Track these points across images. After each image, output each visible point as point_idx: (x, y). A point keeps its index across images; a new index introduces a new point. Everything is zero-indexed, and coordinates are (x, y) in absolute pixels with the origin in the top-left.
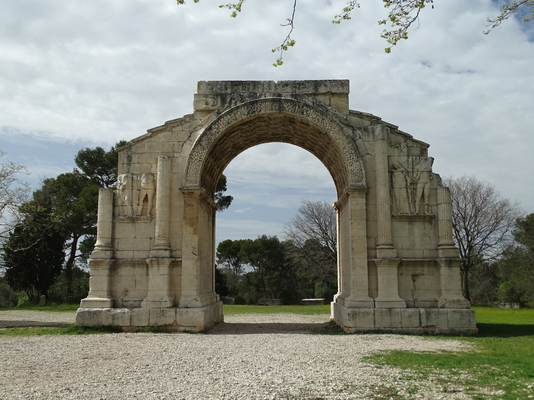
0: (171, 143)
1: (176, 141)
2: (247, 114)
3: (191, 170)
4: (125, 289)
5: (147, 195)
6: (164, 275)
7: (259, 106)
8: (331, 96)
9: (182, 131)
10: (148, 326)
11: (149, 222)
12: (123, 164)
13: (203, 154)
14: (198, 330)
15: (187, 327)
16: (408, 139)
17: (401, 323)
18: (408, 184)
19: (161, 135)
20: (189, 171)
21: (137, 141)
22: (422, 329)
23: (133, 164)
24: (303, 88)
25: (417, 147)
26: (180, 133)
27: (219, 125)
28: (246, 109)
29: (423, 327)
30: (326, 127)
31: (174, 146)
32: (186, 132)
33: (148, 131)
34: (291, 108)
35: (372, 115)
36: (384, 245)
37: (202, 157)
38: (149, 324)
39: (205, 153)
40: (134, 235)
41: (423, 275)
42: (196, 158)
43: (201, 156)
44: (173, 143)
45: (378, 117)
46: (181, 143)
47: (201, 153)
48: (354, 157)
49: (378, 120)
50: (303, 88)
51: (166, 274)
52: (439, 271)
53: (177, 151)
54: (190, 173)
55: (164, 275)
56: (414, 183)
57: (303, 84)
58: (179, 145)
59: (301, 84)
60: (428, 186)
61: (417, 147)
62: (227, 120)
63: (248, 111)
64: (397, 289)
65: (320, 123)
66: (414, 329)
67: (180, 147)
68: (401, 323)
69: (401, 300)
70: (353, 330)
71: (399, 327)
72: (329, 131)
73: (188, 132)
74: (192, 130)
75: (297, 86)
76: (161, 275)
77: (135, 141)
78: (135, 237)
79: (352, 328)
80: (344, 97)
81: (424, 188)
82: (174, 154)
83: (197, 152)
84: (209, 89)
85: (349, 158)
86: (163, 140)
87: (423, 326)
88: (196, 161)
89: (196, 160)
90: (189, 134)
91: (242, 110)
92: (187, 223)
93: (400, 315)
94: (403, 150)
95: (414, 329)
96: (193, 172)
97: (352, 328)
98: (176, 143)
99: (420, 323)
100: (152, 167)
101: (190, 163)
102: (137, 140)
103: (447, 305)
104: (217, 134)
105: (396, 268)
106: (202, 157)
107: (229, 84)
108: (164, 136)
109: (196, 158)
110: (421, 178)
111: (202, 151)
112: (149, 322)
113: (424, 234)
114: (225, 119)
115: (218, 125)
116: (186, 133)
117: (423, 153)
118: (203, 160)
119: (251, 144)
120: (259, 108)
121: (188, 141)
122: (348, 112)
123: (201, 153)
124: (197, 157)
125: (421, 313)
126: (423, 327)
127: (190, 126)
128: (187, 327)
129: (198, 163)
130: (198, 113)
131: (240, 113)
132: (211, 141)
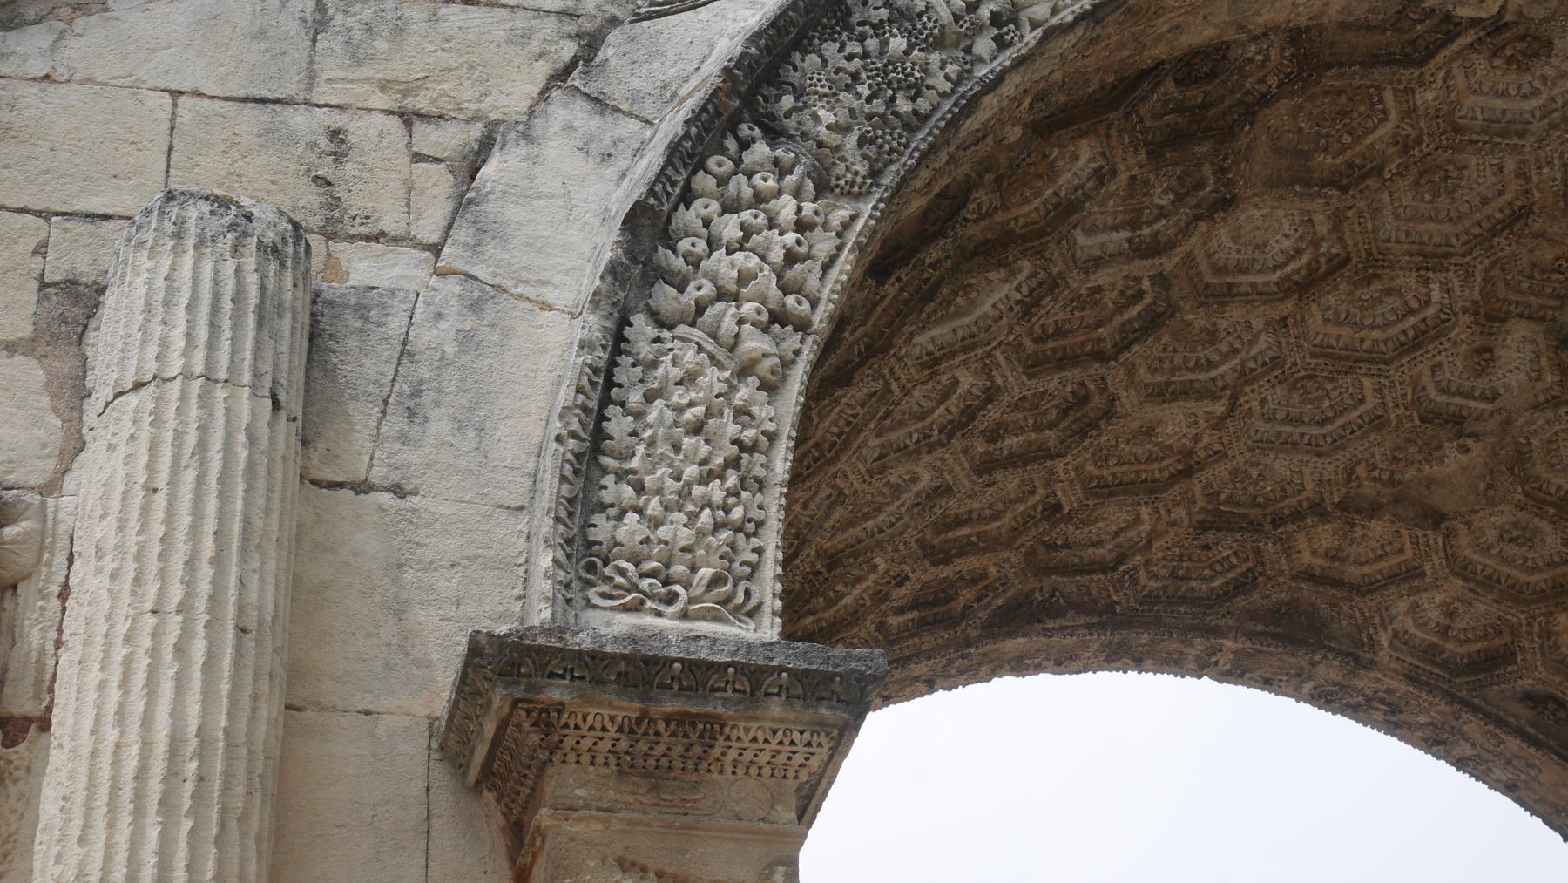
0: (299, 119)
1: (380, 101)
13: (823, 245)
20: (619, 425)
31: (338, 157)
32: (521, 21)
37: (807, 273)
39: (852, 237)
42: (724, 266)
46: (451, 139)
53: (391, 222)
58: (418, 157)
67: (438, 184)
101: (641, 327)
104: (984, 45)
106: (807, 273)
109: (724, 266)
111: (797, 194)
116: (526, 36)
118: (820, 319)
119: (927, 641)
121: (566, 111)
129: (754, 343)
132: (923, 105)
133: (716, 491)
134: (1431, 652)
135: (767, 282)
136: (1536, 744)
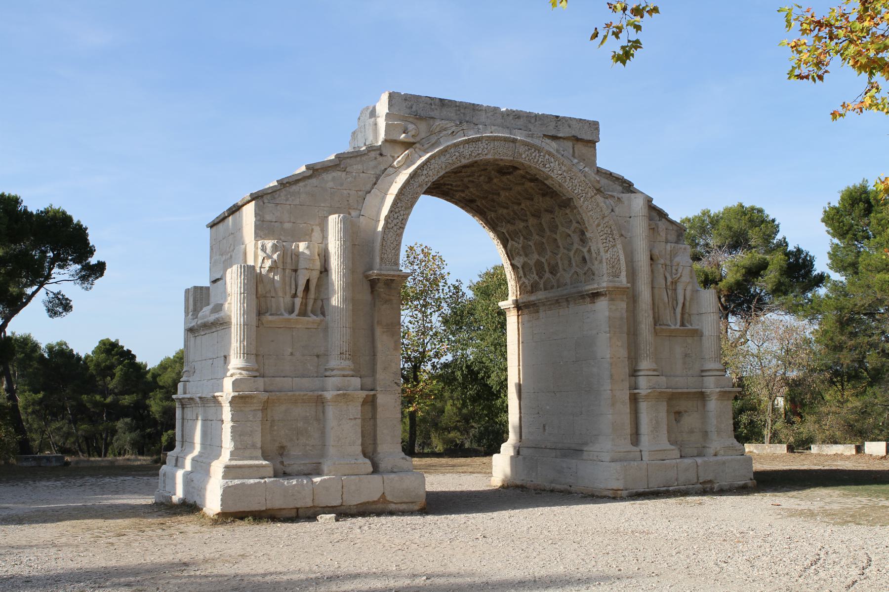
2: (468, 156)
3: (389, 241)
4: (280, 443)
5: (308, 281)
6: (355, 419)
7: (486, 146)
8: (575, 142)
9: (363, 172)
10: (341, 505)
11: (316, 327)
12: (263, 221)
14: (416, 508)
15: (401, 503)
16: (663, 217)
17: (677, 480)
18: (669, 284)
19: (328, 176)
21: (287, 183)
22: (700, 486)
23: (281, 222)
24: (541, 125)
25: (673, 230)
26: (359, 176)
27: (428, 170)
28: (467, 148)
29: (700, 483)
30: (574, 190)
31: (349, 197)
33: (308, 167)
34: (529, 155)
35: (623, 177)
36: (647, 370)
38: (342, 502)
40: (290, 350)
41: (686, 412)
43: (402, 220)
44: (349, 191)
45: (631, 182)
47: (402, 214)
48: (611, 239)
49: (630, 185)
50: (541, 125)
51: (359, 418)
52: (704, 406)
54: (386, 248)
55: (355, 419)
56: (675, 283)
57: (540, 119)
59: (538, 119)
60: (689, 288)
61: (673, 230)
62: (440, 163)
63: (470, 153)
64: (666, 432)
65: (567, 183)
66: (691, 486)
68: (677, 480)
69: (673, 447)
70: (625, 493)
71: (675, 484)
72: (579, 196)
73: (372, 176)
74: (378, 172)
75: (533, 121)
76: (350, 419)
77: (285, 182)
78: (292, 354)
79: (622, 490)
80: (591, 147)
81: (685, 290)
82: (350, 211)
83: (396, 213)
84: (406, 107)
85: (605, 241)
86: (330, 184)
87: (701, 481)
88: (395, 228)
89: (395, 225)
90: (375, 180)
91: (462, 150)
92: (384, 332)
93: (675, 468)
94: (661, 234)
95: (691, 486)
96: (392, 245)
97: (622, 490)
98: (353, 192)
99: (698, 479)
100: (312, 230)
102: (287, 181)
103: (722, 452)
105: (666, 403)
107: (437, 101)
108: (334, 179)
110: (683, 275)
112: (342, 499)
113: (686, 355)
114: (436, 162)
115: (426, 170)
117: (680, 240)
120: (485, 150)
122: (596, 170)
123: (402, 214)
124: (397, 221)
125: (699, 464)
126: (700, 483)
127: (375, 167)
128: (401, 503)
130: (387, 144)
131: (458, 155)
133: (394, 251)
134: (464, 198)
135: (399, 224)
136: (477, 212)
